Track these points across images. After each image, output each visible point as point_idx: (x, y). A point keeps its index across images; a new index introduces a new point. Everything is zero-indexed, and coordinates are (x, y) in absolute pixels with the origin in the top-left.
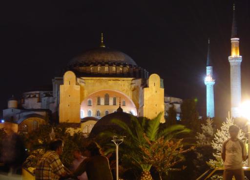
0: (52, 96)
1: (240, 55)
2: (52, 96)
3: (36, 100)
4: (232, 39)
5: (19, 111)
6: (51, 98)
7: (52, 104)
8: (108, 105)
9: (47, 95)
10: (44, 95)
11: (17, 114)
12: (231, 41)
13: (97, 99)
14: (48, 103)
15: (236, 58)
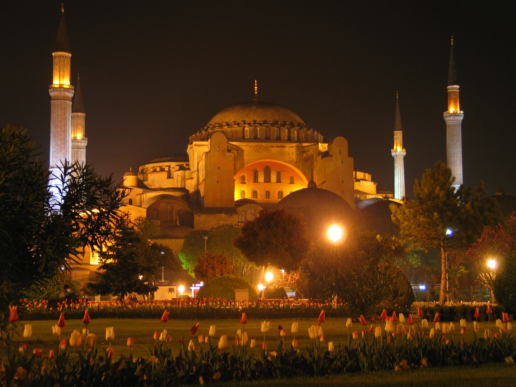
0: (189, 169)
1: (461, 109)
2: (189, 169)
3: (165, 175)
4: (448, 87)
5: (140, 191)
6: (187, 172)
7: (189, 181)
8: (270, 182)
9: (182, 168)
10: (178, 168)
11: (137, 195)
12: (447, 90)
13: (252, 173)
14: (184, 179)
15: (455, 114)
